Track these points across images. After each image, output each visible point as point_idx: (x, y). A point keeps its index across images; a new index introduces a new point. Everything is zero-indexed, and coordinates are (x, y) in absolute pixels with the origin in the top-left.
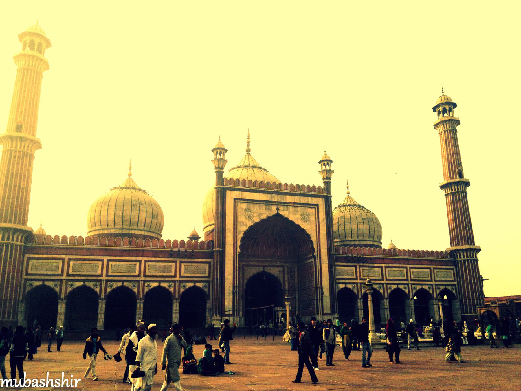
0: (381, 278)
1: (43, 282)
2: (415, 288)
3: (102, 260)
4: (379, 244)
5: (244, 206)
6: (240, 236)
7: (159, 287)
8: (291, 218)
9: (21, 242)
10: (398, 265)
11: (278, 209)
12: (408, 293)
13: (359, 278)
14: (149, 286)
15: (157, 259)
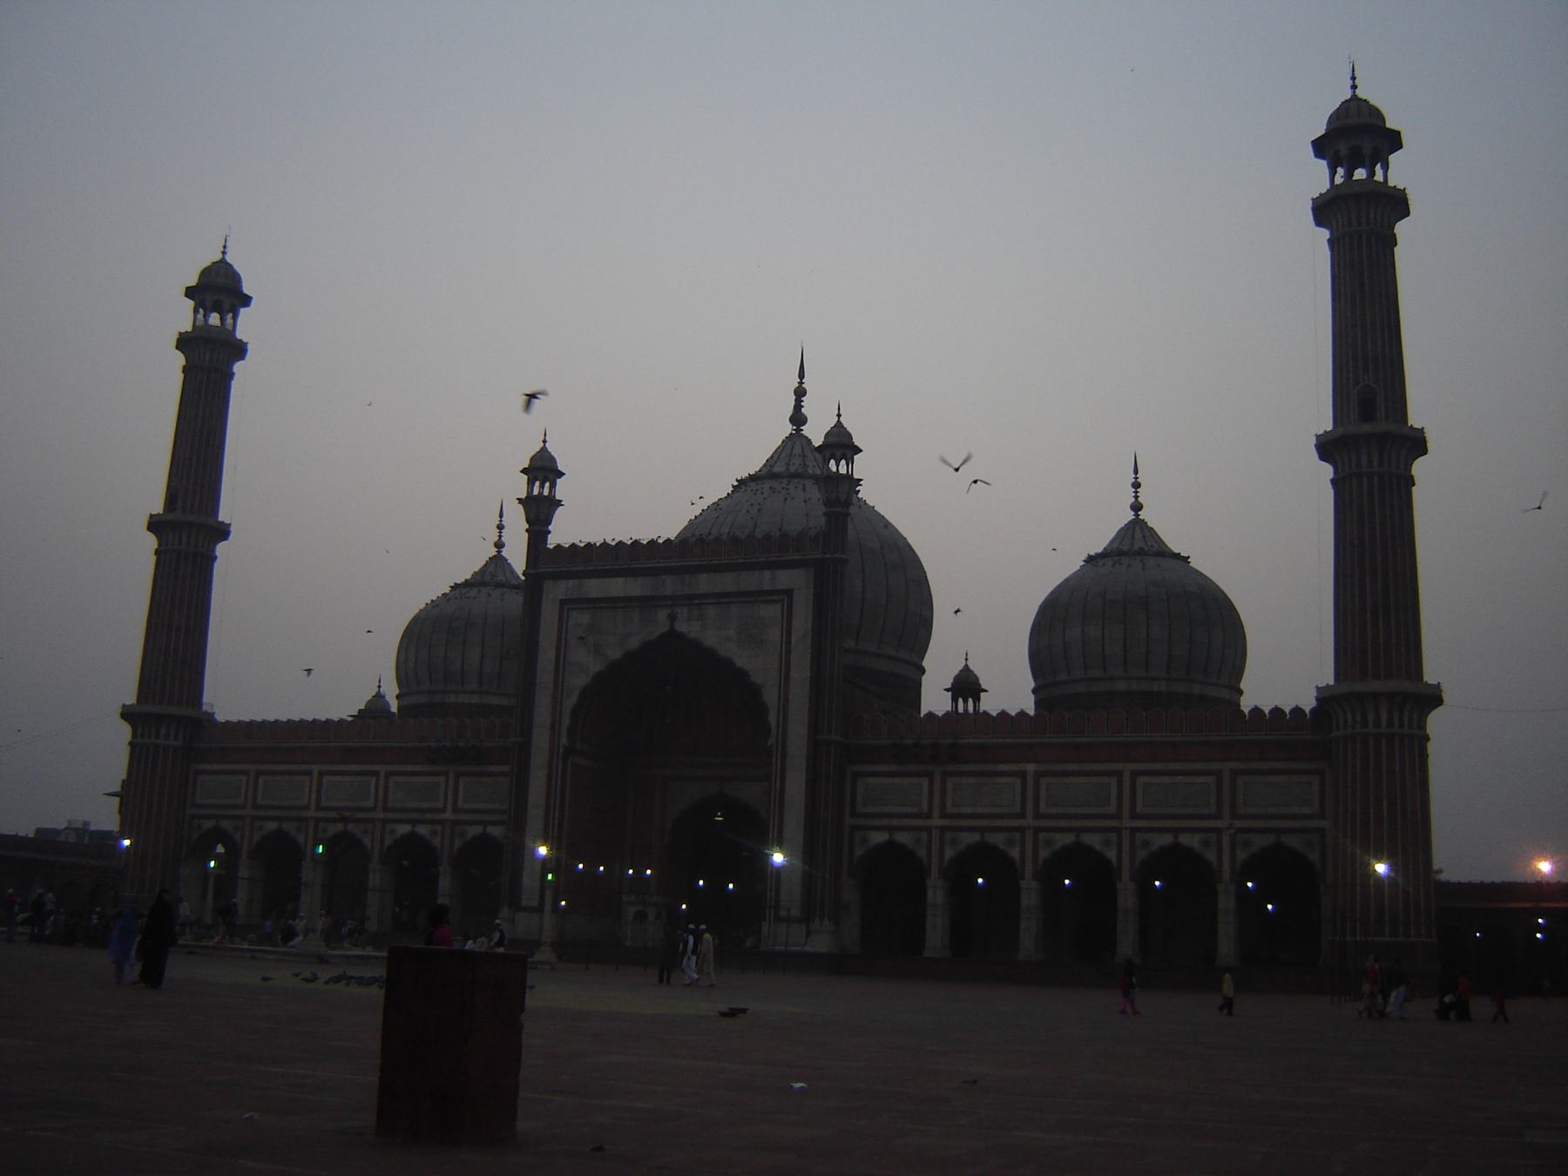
0: (1018, 809)
1: (218, 821)
2: (1146, 844)
3: (309, 773)
4: (1197, 689)
5: (584, 618)
6: (570, 702)
7: (413, 835)
8: (711, 639)
9: (176, 738)
10: (1086, 767)
11: (672, 618)
12: (1114, 860)
13: (936, 813)
14: (393, 831)
15: (410, 768)
